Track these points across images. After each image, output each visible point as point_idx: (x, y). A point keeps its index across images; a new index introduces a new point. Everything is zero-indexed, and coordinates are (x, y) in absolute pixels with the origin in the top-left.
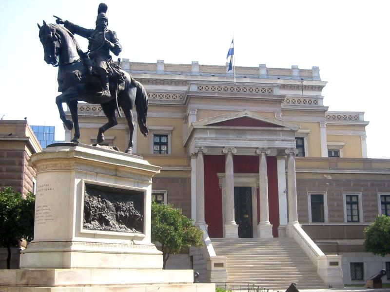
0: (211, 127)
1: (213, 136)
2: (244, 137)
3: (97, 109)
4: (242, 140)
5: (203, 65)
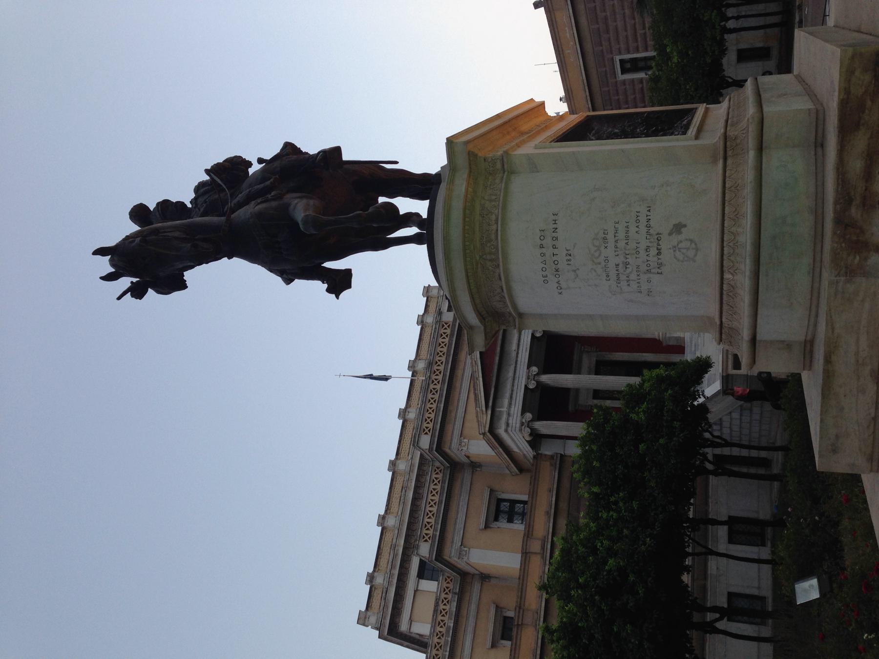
0: (490, 404)
1: (506, 402)
2: (514, 354)
3: (441, 630)
4: (517, 357)
5: (397, 454)
